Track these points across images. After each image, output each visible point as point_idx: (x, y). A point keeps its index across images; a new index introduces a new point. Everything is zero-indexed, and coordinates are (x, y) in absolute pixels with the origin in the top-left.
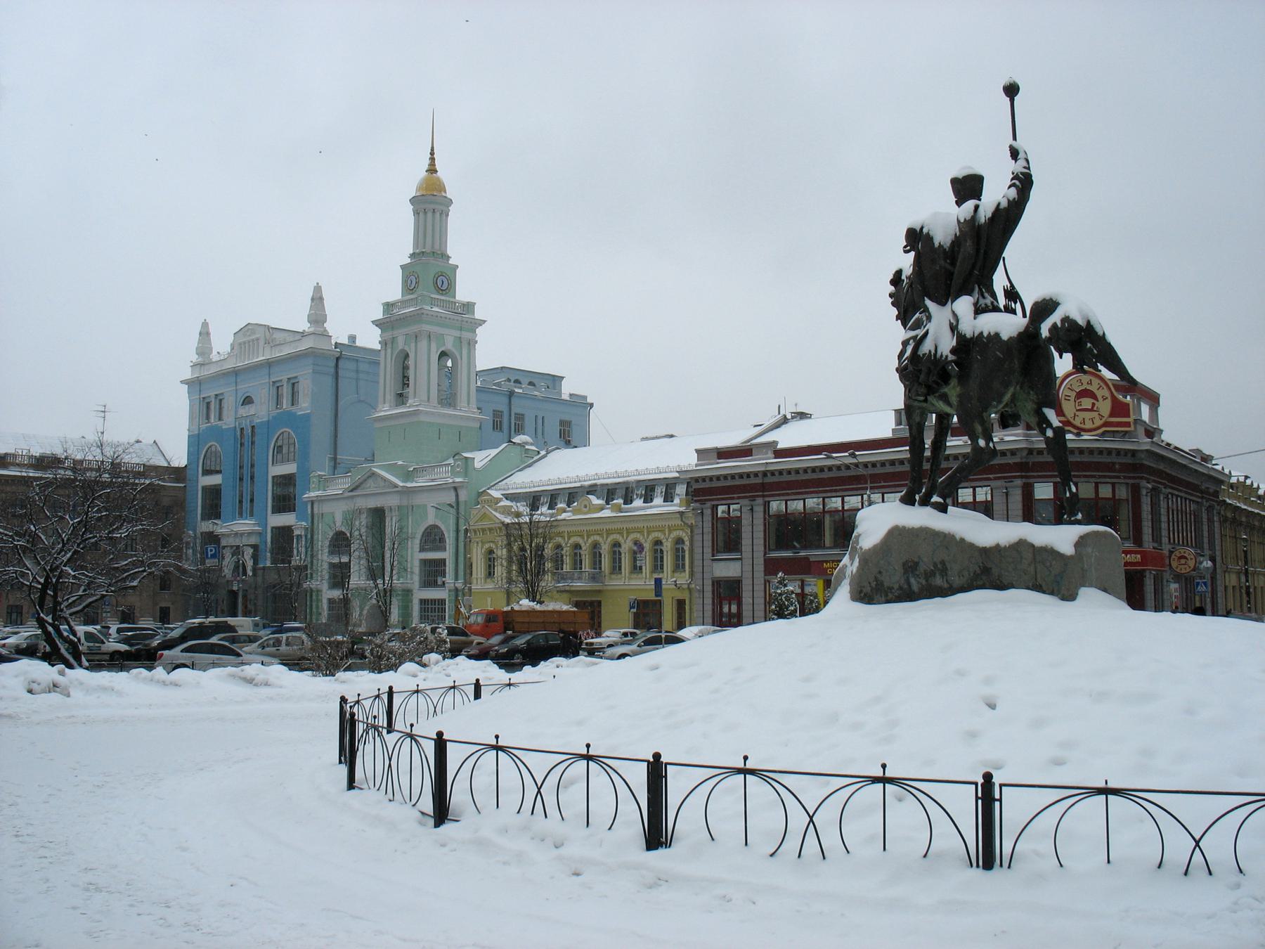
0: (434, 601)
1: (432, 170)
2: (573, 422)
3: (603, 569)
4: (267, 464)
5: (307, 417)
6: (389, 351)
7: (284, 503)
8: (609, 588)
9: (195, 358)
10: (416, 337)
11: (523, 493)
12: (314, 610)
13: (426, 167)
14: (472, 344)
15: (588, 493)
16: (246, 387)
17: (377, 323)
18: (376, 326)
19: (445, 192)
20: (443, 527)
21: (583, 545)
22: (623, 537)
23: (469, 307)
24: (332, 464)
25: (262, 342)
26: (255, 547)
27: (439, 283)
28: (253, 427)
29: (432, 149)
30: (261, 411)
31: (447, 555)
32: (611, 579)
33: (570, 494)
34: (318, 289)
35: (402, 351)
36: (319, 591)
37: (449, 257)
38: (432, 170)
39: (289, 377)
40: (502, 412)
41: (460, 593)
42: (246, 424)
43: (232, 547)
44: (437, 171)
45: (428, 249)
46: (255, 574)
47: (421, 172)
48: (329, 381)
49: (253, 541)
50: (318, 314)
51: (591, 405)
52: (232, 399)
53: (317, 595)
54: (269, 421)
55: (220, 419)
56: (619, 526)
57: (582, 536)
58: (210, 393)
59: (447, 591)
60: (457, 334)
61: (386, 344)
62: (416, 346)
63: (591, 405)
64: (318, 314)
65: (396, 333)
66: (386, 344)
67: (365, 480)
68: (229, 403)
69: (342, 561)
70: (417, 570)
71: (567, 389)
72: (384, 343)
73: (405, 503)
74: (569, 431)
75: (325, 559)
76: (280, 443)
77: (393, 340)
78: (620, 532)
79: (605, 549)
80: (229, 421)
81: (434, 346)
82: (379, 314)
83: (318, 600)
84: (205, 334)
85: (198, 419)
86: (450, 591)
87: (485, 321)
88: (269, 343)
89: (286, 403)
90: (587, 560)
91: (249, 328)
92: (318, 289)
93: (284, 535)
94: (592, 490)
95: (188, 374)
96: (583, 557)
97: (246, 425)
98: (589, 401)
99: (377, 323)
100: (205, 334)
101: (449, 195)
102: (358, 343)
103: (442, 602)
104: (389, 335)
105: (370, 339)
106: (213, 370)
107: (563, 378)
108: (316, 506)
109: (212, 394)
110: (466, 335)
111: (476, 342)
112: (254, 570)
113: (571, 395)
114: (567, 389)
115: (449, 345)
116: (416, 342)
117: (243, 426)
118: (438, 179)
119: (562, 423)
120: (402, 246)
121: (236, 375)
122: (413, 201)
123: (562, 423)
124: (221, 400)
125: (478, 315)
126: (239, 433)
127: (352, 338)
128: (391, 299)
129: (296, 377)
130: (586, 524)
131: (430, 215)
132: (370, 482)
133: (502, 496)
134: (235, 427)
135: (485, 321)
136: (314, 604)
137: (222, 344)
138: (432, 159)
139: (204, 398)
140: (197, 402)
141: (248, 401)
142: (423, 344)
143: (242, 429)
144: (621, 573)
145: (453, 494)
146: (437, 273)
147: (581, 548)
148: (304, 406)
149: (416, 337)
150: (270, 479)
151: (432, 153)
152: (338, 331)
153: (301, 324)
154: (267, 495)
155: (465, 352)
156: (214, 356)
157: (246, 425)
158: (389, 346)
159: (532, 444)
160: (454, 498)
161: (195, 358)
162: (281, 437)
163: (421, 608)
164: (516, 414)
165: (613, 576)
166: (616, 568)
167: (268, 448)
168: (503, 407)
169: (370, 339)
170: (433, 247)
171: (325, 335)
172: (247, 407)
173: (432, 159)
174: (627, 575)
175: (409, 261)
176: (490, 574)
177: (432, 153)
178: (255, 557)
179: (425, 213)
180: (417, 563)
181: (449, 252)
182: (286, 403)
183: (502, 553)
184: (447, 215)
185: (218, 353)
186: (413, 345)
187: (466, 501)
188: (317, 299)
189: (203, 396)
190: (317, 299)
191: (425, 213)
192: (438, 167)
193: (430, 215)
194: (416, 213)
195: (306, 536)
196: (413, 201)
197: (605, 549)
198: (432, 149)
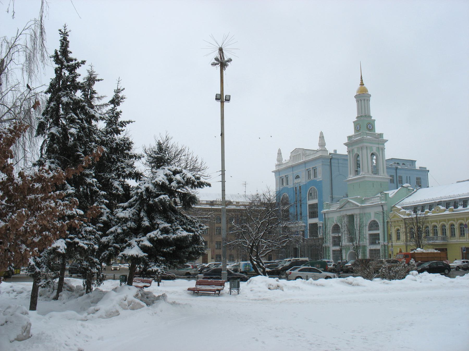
0: (375, 250)
1: (362, 84)
2: (421, 178)
3: (447, 235)
5: (321, 182)
6: (351, 154)
7: (314, 214)
8: (450, 243)
9: (276, 163)
10: (362, 148)
11: (410, 206)
12: (327, 254)
13: (360, 83)
14: (383, 149)
15: (438, 205)
16: (296, 172)
17: (346, 144)
18: (346, 145)
19: (368, 92)
20: (378, 221)
21: (437, 226)
22: (446, 222)
23: (381, 135)
24: (331, 199)
25: (301, 155)
26: (303, 232)
27: (369, 127)
28: (300, 187)
29: (361, 76)
30: (303, 180)
31: (380, 232)
32: (450, 239)
33: (430, 205)
34: (321, 133)
35: (357, 154)
37: (371, 117)
38: (362, 84)
39: (313, 167)
40: (393, 176)
41: (386, 247)
42: (297, 186)
44: (364, 85)
45: (363, 115)
47: (358, 86)
48: (328, 168)
50: (322, 143)
51: (428, 171)
52: (292, 177)
53: (328, 249)
54: (306, 184)
55: (287, 184)
56: (453, 217)
57: (437, 222)
58: (283, 175)
59: (381, 246)
60: (377, 146)
61: (350, 152)
62: (362, 152)
63: (428, 171)
64: (322, 143)
65: (353, 147)
66: (350, 152)
67: (345, 204)
68: (291, 178)
69: (339, 235)
70: (368, 238)
71: (418, 166)
72: (349, 152)
73: (361, 212)
74: (420, 182)
75: (331, 235)
76: (311, 192)
77: (353, 150)
78: (445, 221)
79: (447, 227)
80: (291, 185)
81: (369, 151)
82: (346, 141)
83: (329, 251)
84: (280, 154)
85: (279, 185)
86: (382, 246)
87: (387, 140)
88: (304, 155)
89: (312, 177)
90: (440, 232)
91: (296, 150)
92: (321, 133)
93: (314, 227)
94: (440, 203)
95: (274, 169)
96: (438, 230)
97: (297, 186)
98: (427, 169)
99: (346, 144)
100: (280, 154)
101: (369, 93)
102: (338, 153)
103: (379, 250)
104: (351, 148)
105: (343, 150)
106: (284, 166)
107: (416, 161)
108: (326, 215)
109: (284, 175)
110: (381, 146)
111: (385, 149)
113: (420, 167)
114: (418, 166)
115: (374, 151)
116: (362, 150)
117: (296, 186)
118: (365, 88)
119: (418, 179)
120: (353, 115)
121: (305, 164)
122: (356, 97)
123: (418, 179)
124: (287, 178)
125: (385, 138)
126: (295, 189)
127: (335, 151)
128: (350, 135)
129: (316, 167)
130: (455, 216)
131: (363, 101)
132: (347, 205)
133: (401, 208)
134: (293, 187)
135: (387, 140)
136: (327, 252)
137: (286, 157)
138: (362, 80)
139: (281, 177)
140: (278, 179)
141: (297, 177)
142: (365, 151)
143: (296, 188)
144: (455, 237)
145: (381, 208)
146: (368, 123)
147: (436, 227)
148: (320, 177)
149: (362, 148)
150: (308, 206)
151: (361, 78)
152: (330, 149)
153: (316, 147)
154: (307, 212)
155: (381, 152)
156: (284, 162)
157: (297, 186)
158: (351, 152)
159: (410, 187)
160: (382, 209)
161: (276, 163)
162: (311, 190)
163: (370, 253)
164: (399, 176)
165: (452, 238)
166: (453, 235)
167: (306, 194)
168: (394, 174)
169: (343, 150)
170: (365, 113)
171: (326, 151)
172: (297, 179)
173: (362, 80)
174: (458, 237)
175: (356, 120)
176: (398, 238)
177: (361, 78)
178: (303, 235)
179: (361, 101)
180: (367, 235)
181: (371, 115)
182: (312, 177)
183: (402, 230)
184: (370, 101)
185: (285, 160)
186: (361, 151)
187: (387, 211)
188: (322, 137)
189: (281, 176)
190: (322, 137)
191: (361, 101)
192: (364, 83)
193: (363, 101)
194: (357, 101)
195: (323, 227)
196: (356, 97)
197: (447, 227)
198: (361, 76)
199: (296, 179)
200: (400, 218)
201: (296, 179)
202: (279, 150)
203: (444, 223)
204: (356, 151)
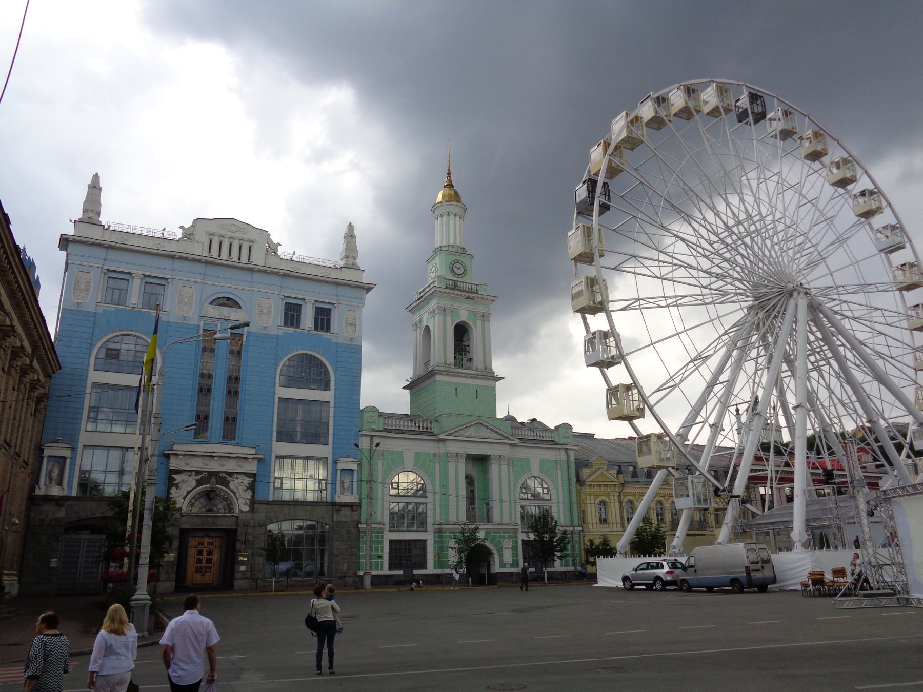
4: (275, 383)
6: (449, 319)
29: (449, 170)
36: (381, 531)
43: (198, 473)
46: (252, 509)
49: (252, 467)
57: (664, 497)
61: (444, 310)
95: (70, 230)
112: (253, 502)
132: (472, 429)
134: (199, 326)
149: (483, 316)
150: (276, 400)
151: (449, 174)
177: (449, 174)
178: (252, 487)
189: (110, 268)
198: (449, 170)
199: (210, 304)
200: (613, 481)
201: (210, 304)
202: (96, 177)
203: (632, 498)
204: (463, 317)
